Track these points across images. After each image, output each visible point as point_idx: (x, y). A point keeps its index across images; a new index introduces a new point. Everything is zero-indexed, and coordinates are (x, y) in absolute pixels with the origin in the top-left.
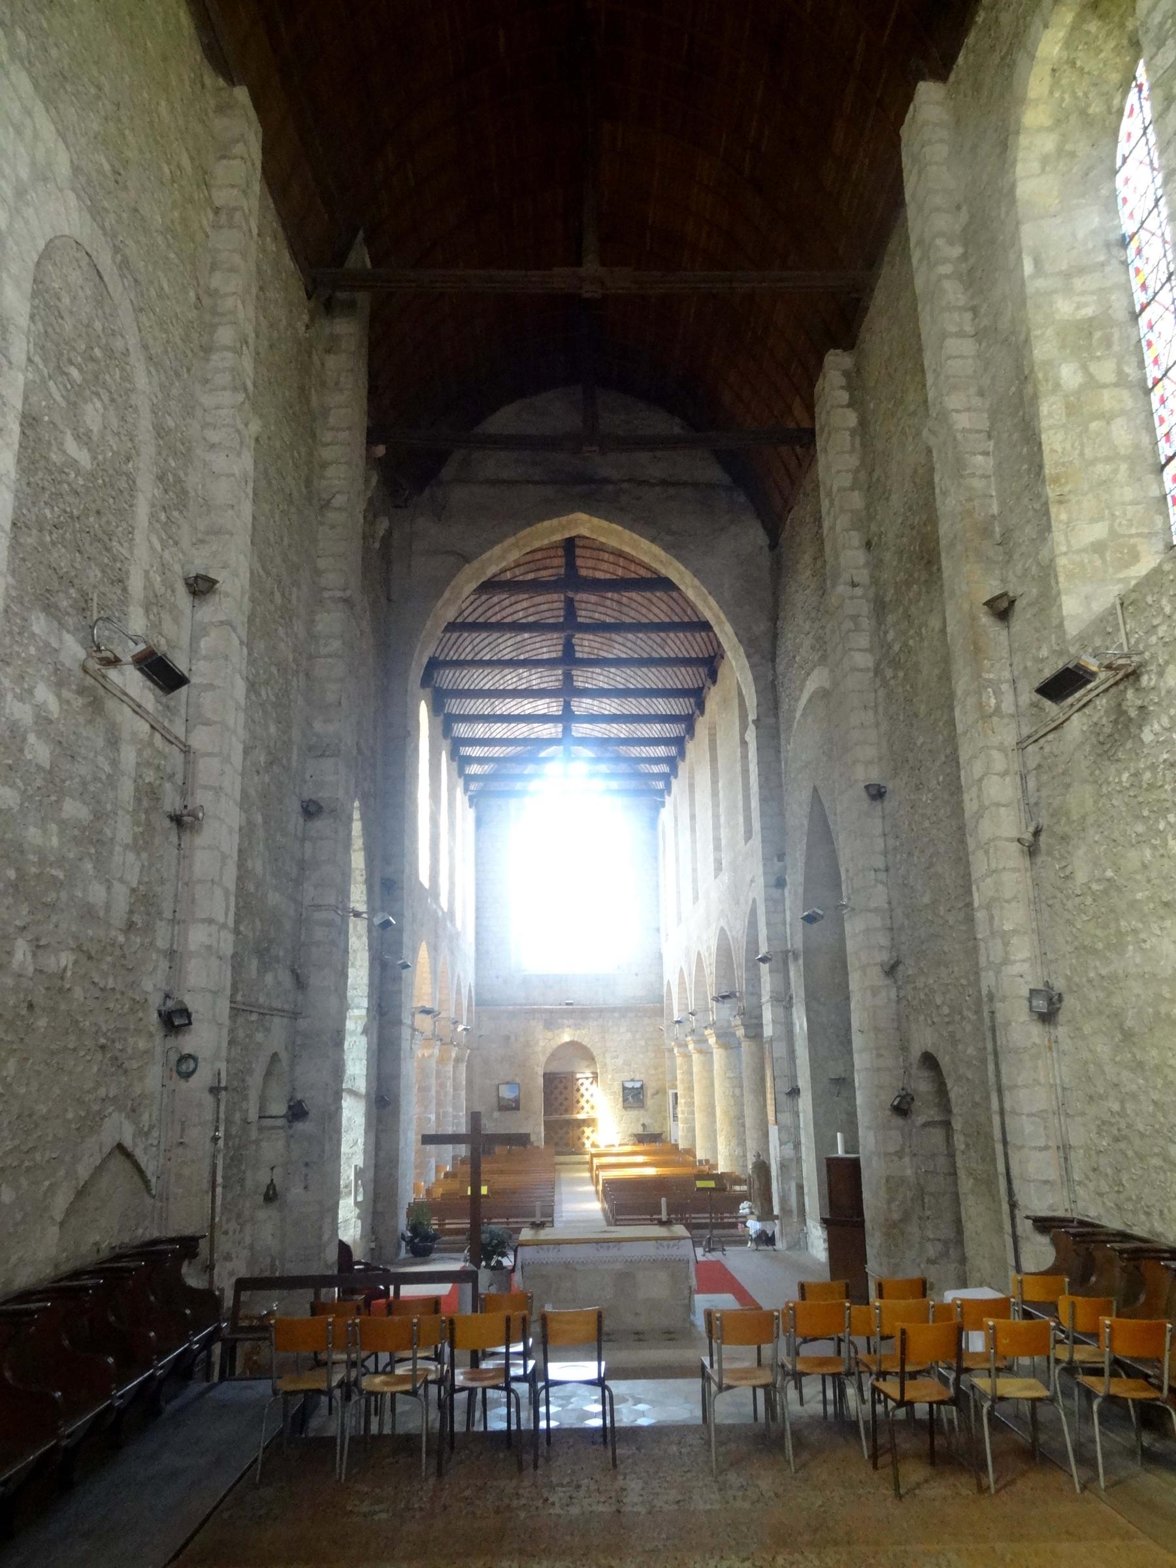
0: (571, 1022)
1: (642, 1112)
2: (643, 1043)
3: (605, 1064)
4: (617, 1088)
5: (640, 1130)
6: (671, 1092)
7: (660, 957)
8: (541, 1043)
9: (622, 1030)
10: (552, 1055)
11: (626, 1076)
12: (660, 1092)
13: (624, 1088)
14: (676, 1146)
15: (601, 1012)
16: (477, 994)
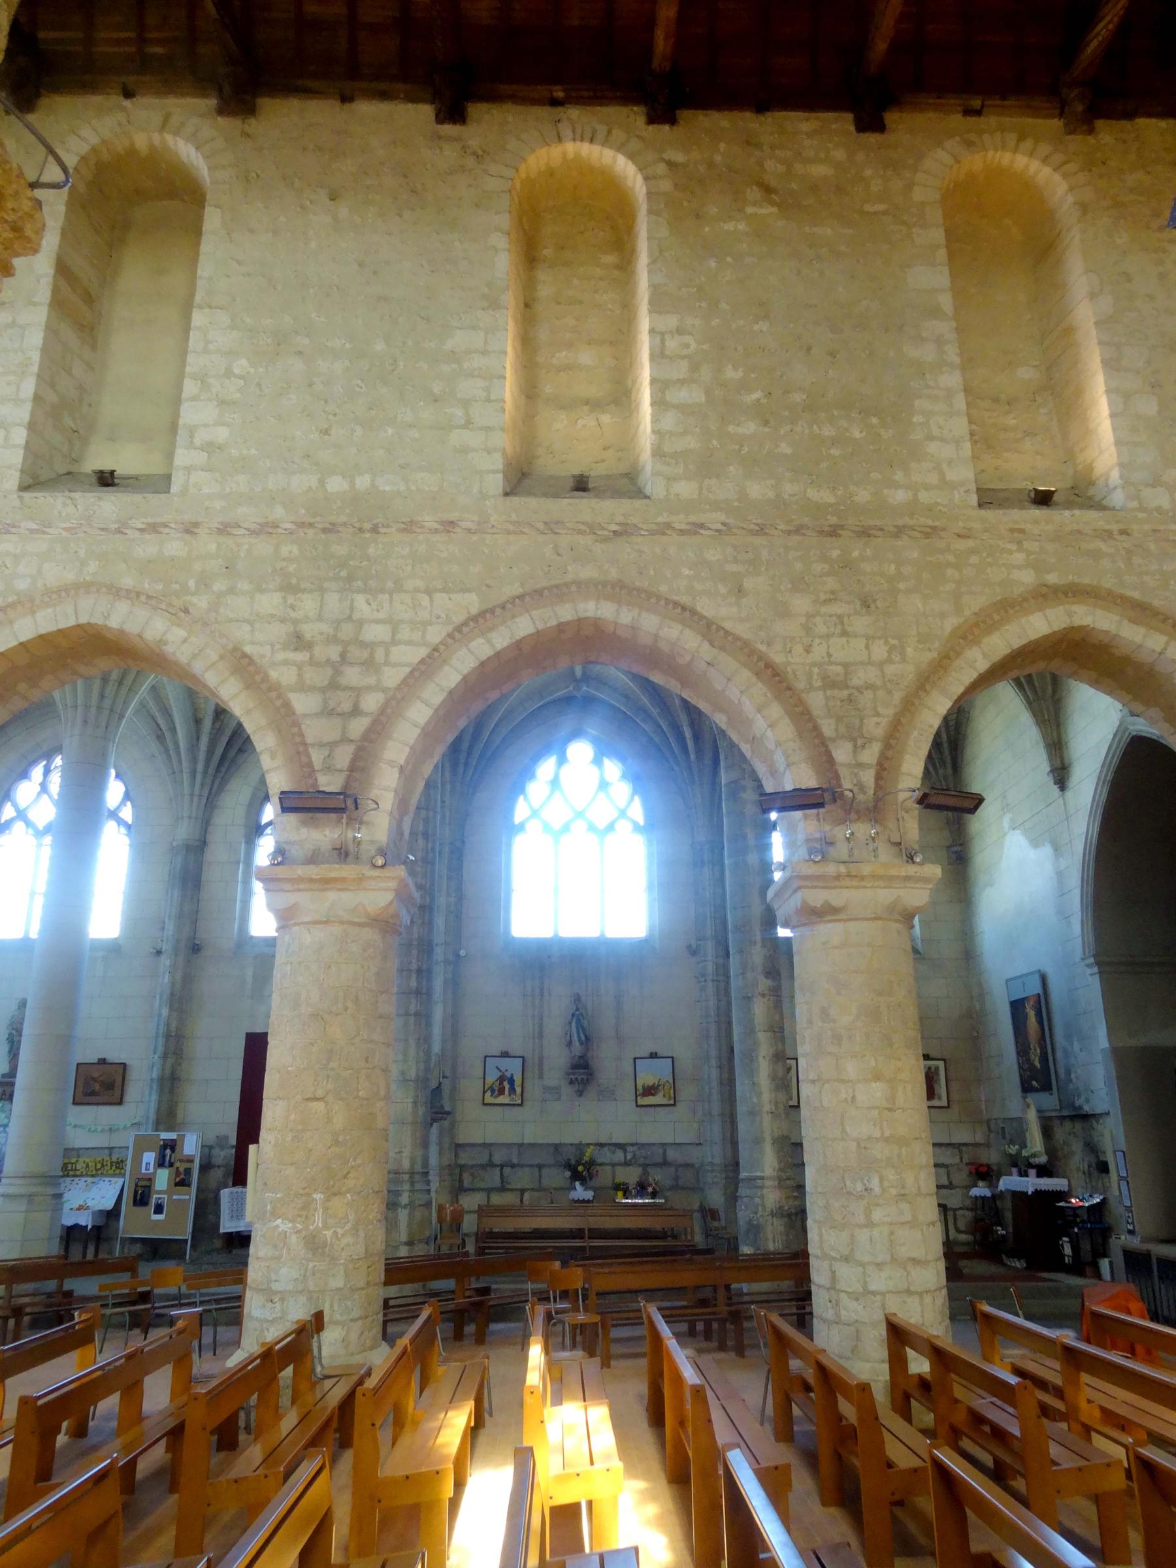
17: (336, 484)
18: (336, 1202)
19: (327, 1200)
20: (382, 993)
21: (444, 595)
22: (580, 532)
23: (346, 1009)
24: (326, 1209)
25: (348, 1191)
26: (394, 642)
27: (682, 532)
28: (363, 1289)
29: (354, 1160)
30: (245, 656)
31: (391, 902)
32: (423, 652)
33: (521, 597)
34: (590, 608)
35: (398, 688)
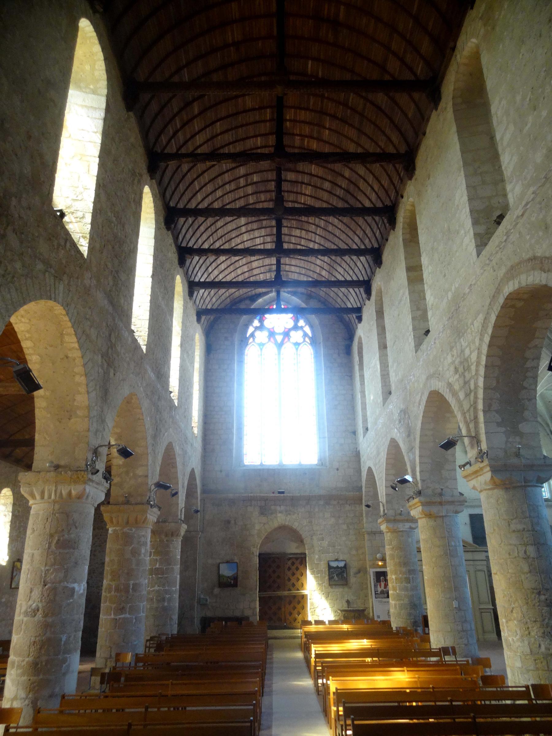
0: (283, 508)
1: (346, 589)
2: (345, 527)
3: (313, 546)
4: (323, 566)
5: (345, 607)
6: (372, 571)
7: (357, 455)
8: (257, 527)
9: (327, 515)
10: (266, 538)
11: (330, 556)
12: (362, 571)
13: (330, 567)
14: (387, 624)
15: (308, 499)
16: (203, 485)
17: (450, 295)
18: (510, 623)
19: (507, 622)
20: (512, 520)
21: (476, 321)
22: (497, 253)
23: (494, 530)
24: (507, 627)
25: (515, 619)
26: (471, 353)
27: (522, 215)
28: (534, 670)
29: (514, 604)
30: (451, 384)
31: (492, 477)
32: (476, 352)
33: (490, 304)
34: (509, 288)
35: (476, 374)
